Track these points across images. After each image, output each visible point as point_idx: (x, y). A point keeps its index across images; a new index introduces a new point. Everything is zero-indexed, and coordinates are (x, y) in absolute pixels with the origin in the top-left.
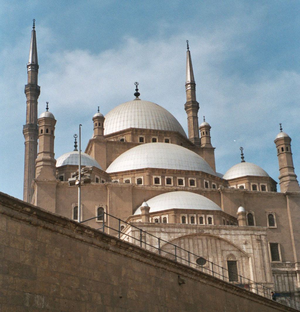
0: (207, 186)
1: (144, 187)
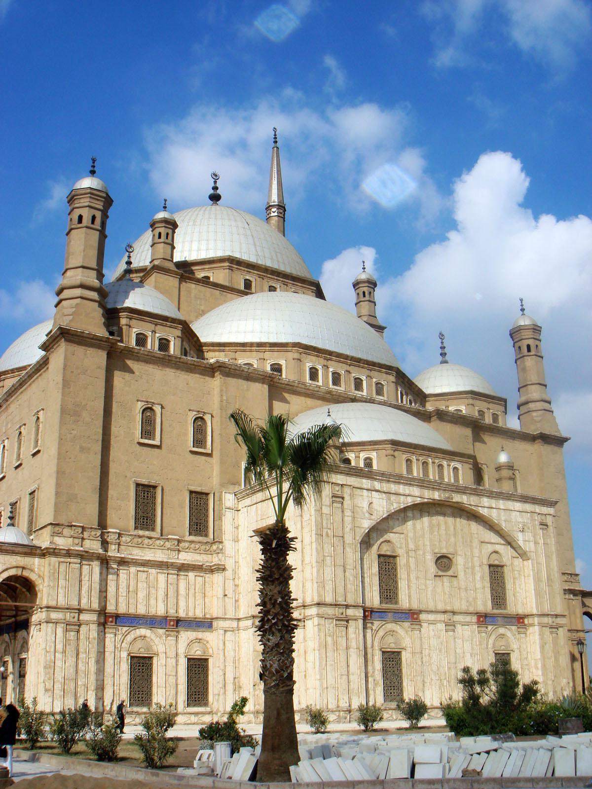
0: (402, 401)
1: (293, 384)
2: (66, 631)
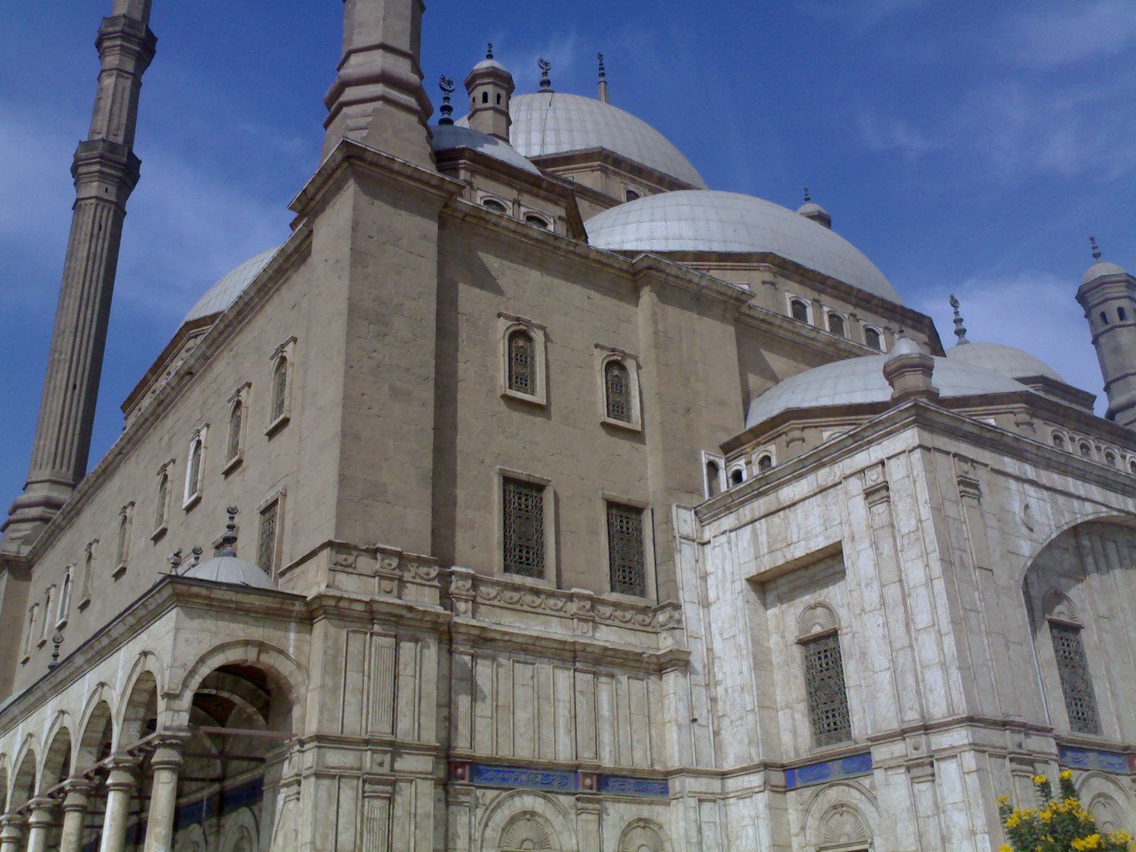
2: (364, 798)
